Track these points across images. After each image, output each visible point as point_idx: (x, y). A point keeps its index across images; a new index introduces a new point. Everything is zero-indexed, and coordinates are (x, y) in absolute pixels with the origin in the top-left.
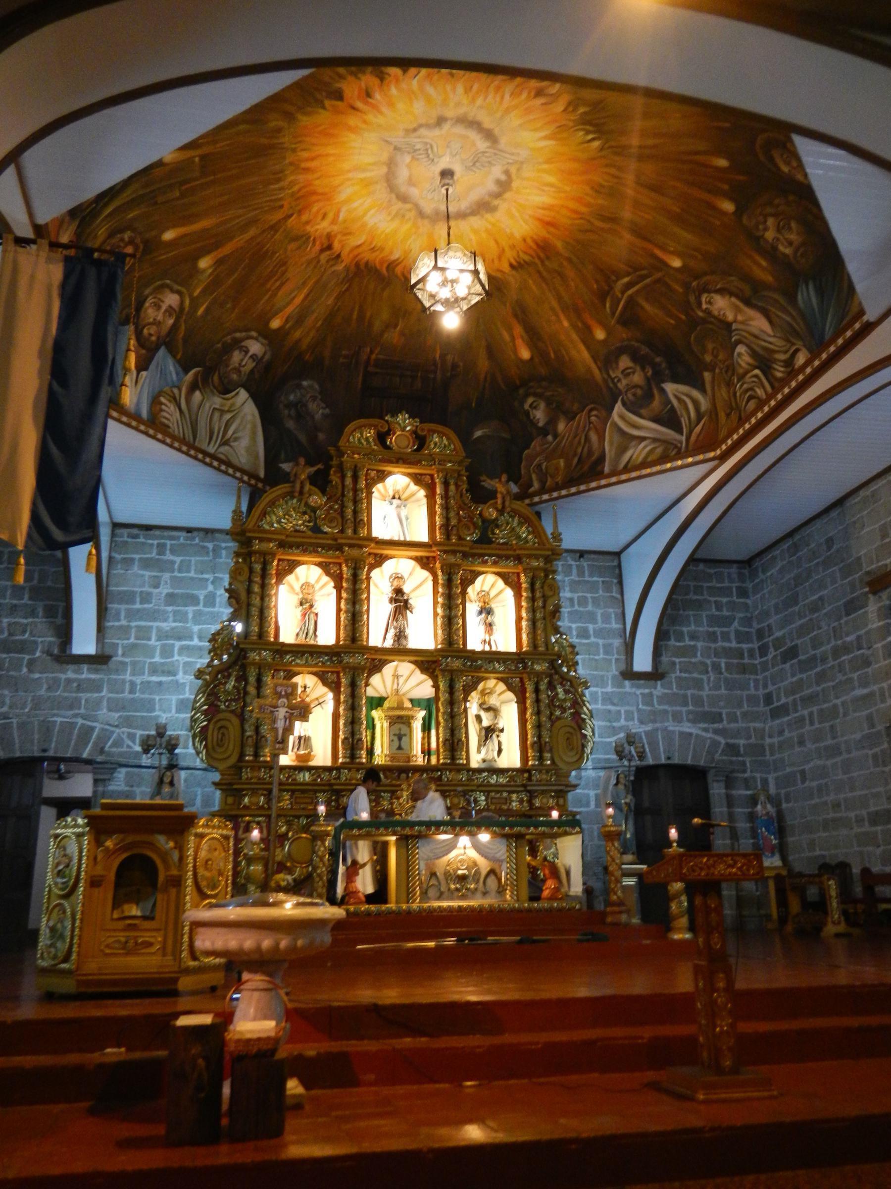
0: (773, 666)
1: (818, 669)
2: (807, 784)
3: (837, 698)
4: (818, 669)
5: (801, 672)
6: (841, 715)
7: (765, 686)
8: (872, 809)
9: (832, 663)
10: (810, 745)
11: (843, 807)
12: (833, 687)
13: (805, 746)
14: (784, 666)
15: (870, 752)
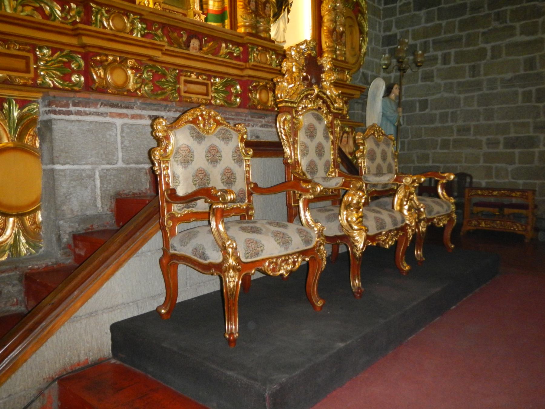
0: (401, 12)
1: (467, 16)
2: (427, 111)
3: (487, 43)
4: (467, 16)
5: (439, 19)
6: (488, 57)
7: (388, 28)
8: (513, 135)
9: (487, 12)
10: (437, 80)
11: (472, 132)
12: (484, 33)
13: (432, 81)
14: (417, 13)
15: (521, 90)
